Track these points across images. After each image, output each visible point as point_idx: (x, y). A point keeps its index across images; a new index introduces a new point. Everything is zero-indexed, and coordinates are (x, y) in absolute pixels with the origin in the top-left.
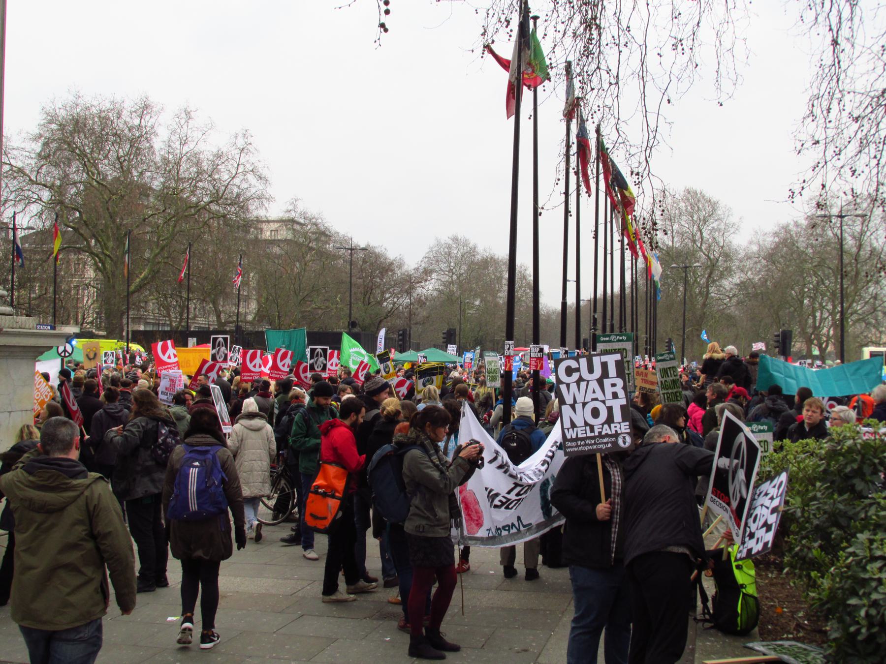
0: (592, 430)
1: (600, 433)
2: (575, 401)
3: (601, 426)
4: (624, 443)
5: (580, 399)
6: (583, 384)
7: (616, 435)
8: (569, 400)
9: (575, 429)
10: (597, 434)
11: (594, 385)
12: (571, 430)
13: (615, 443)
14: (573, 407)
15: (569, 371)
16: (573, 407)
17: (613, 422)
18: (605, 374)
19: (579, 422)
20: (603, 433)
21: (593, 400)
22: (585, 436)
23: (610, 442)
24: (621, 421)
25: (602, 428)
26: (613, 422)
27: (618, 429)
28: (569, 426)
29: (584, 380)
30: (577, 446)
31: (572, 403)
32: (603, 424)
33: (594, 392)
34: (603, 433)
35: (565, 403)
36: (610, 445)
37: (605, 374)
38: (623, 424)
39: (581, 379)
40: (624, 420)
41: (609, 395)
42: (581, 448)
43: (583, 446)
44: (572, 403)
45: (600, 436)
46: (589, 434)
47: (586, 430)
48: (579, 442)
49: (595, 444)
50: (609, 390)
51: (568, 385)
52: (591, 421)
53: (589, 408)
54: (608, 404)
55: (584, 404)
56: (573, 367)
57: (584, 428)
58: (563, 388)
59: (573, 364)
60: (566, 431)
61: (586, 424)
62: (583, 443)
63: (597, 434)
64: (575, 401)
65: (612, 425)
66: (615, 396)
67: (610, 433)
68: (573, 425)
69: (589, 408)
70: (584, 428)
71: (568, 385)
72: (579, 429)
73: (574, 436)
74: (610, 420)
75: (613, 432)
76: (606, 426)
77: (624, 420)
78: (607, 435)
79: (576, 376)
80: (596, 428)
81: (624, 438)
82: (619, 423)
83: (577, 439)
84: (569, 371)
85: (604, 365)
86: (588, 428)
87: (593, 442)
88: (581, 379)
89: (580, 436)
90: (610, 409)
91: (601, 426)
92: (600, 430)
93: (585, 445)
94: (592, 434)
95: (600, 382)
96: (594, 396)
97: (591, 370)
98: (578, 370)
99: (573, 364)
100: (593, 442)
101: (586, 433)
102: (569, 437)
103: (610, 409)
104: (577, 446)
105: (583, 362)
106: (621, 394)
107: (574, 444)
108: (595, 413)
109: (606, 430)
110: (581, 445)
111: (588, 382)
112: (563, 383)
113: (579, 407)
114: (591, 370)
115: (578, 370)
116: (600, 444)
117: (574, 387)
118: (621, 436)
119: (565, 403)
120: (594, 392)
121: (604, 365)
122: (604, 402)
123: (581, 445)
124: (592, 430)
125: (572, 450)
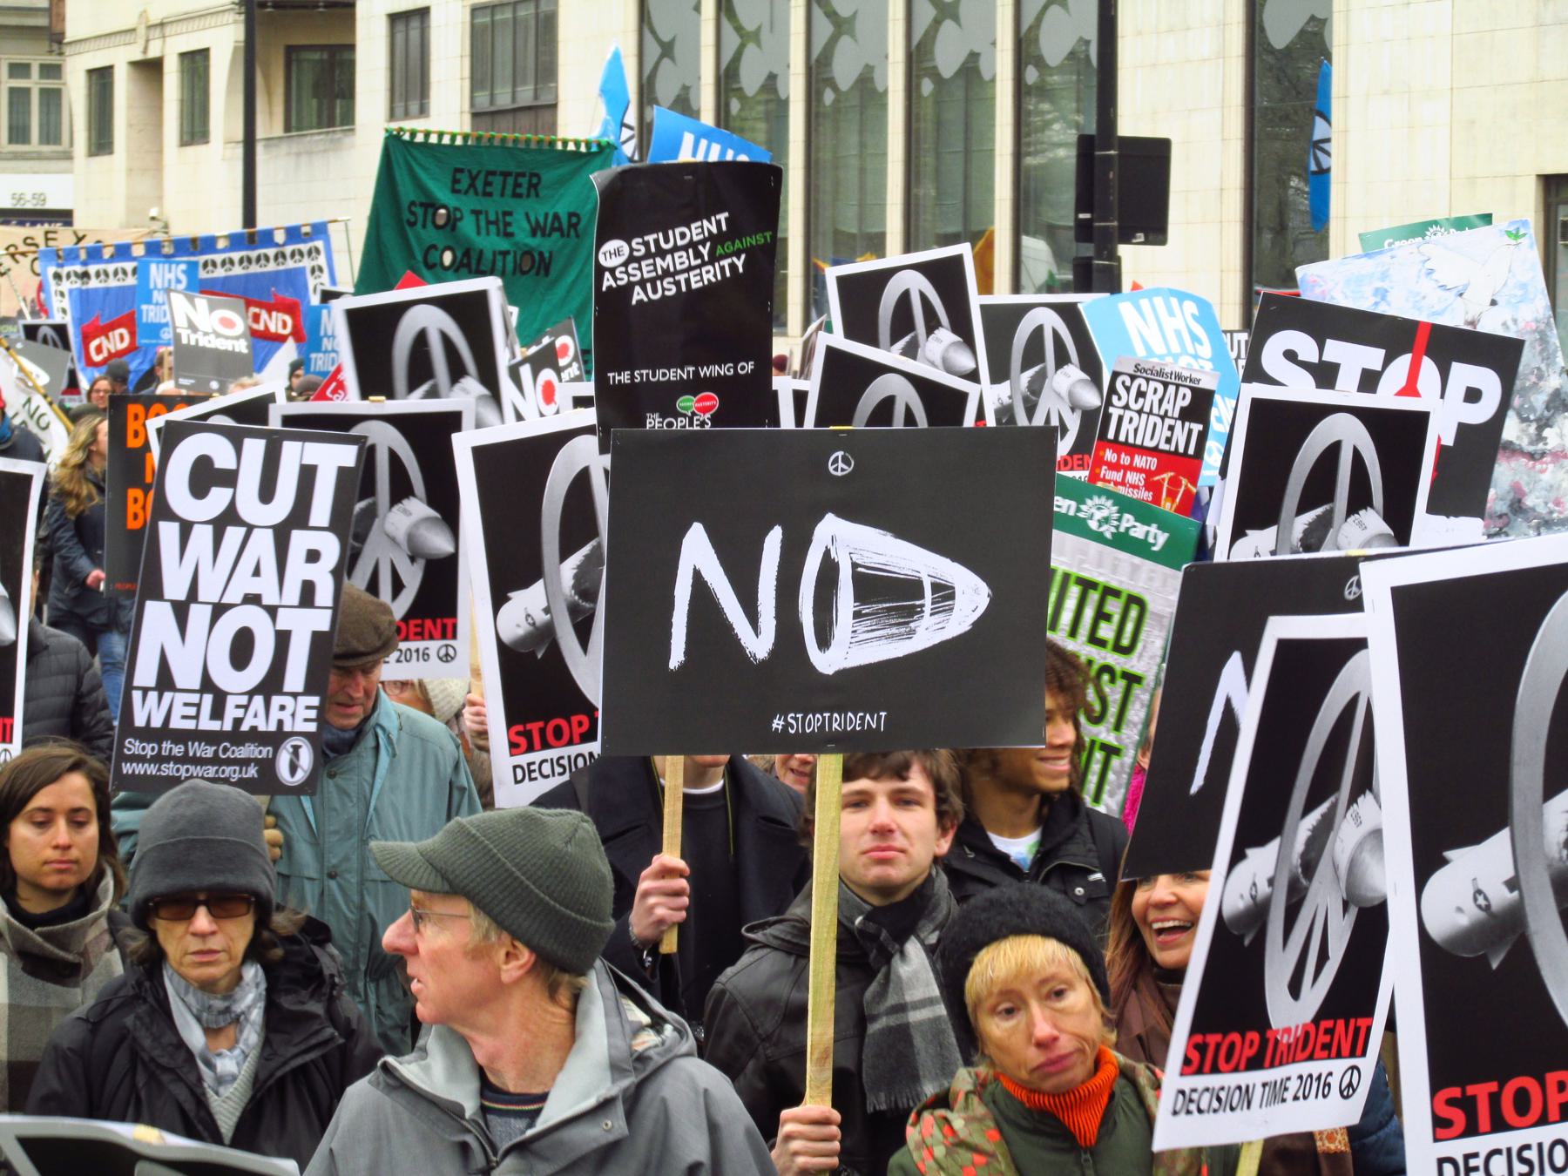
0: (217, 712)
1: (238, 722)
3: (244, 700)
4: (293, 768)
5: (209, 591)
6: (234, 534)
7: (276, 738)
8: (175, 584)
9: (168, 696)
10: (228, 726)
11: (263, 544)
12: (153, 695)
14: (181, 611)
15: (205, 477)
16: (181, 611)
17: (280, 692)
19: (186, 675)
20: (245, 727)
22: (190, 725)
23: (257, 761)
24: (300, 688)
25: (246, 707)
26: (279, 690)
27: (286, 716)
28: (152, 683)
30: (159, 759)
32: (251, 694)
33: (257, 572)
34: (245, 727)
35: (158, 596)
36: (252, 772)
39: (230, 517)
40: (309, 690)
41: (293, 593)
43: (177, 760)
44: (181, 596)
45: (237, 736)
46: (207, 724)
47: (198, 706)
48: (166, 745)
50: (298, 571)
51: (186, 528)
52: (225, 676)
55: (219, 610)
56: (219, 464)
57: (195, 698)
58: (168, 532)
60: (137, 696)
61: (207, 685)
62: (178, 750)
63: (228, 726)
65: (276, 700)
66: (307, 595)
67: (262, 728)
68: (165, 681)
70: (195, 698)
71: (186, 528)
72: (181, 698)
73: (157, 723)
74: (272, 685)
75: (273, 727)
76: (258, 701)
77: (309, 690)
78: (255, 736)
79: (218, 499)
80: (231, 702)
81: (296, 749)
82: (295, 695)
83: (165, 733)
84: (205, 477)
85: (308, 475)
86: (208, 699)
87: (209, 752)
88: (230, 517)
89: (176, 723)
90: (283, 639)
92: (240, 713)
94: (215, 726)
95: (282, 535)
96: (254, 586)
97: (267, 492)
99: (220, 452)
100: (209, 752)
101: (197, 717)
102: (140, 721)
103: (283, 639)
105: (255, 449)
106: (324, 595)
107: (149, 750)
109: (257, 718)
110: (170, 758)
111: (250, 528)
112: (171, 516)
113: (199, 615)
114: (267, 492)
115: (229, 478)
116: (229, 762)
117: (202, 537)
119: (158, 596)
120: (257, 572)
121: (308, 475)
122: (272, 611)
123: (170, 758)
124: (217, 712)
125: (140, 769)
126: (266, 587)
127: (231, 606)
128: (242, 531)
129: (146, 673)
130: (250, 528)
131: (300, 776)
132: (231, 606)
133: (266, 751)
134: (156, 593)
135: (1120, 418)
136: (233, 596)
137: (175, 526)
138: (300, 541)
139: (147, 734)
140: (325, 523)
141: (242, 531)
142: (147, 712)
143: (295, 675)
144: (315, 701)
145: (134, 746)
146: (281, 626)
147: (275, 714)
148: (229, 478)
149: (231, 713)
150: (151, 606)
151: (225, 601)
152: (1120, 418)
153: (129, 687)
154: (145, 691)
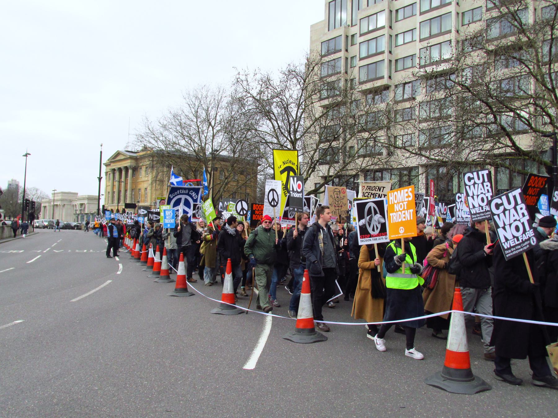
0: (518, 240)
1: (522, 240)
3: (522, 236)
5: (507, 223)
6: (507, 212)
9: (508, 242)
10: (521, 241)
11: (513, 211)
12: (506, 243)
13: (530, 244)
14: (504, 228)
16: (504, 228)
18: (516, 204)
19: (510, 237)
20: (524, 240)
21: (515, 220)
22: (514, 244)
23: (528, 244)
27: (529, 235)
28: (504, 241)
29: (507, 210)
31: (503, 225)
32: (522, 235)
33: (514, 216)
34: (524, 240)
36: (528, 246)
37: (516, 204)
38: (530, 231)
39: (505, 210)
41: (521, 216)
42: (514, 253)
43: (515, 251)
44: (503, 225)
46: (517, 243)
47: (514, 241)
48: (512, 249)
49: (522, 247)
50: (520, 212)
51: (498, 215)
52: (516, 234)
53: (513, 226)
54: (522, 221)
55: (510, 225)
57: (513, 240)
58: (496, 217)
59: (498, 201)
60: (503, 244)
61: (514, 237)
62: (514, 249)
66: (523, 215)
67: (526, 239)
68: (507, 240)
69: (513, 226)
70: (513, 240)
72: (510, 241)
73: (509, 247)
74: (525, 231)
75: (528, 238)
76: (524, 235)
77: (530, 229)
78: (526, 240)
79: (501, 208)
80: (519, 238)
82: (529, 231)
83: (511, 247)
84: (498, 206)
86: (515, 239)
87: (520, 247)
88: (505, 210)
89: (512, 245)
90: (523, 224)
91: (522, 236)
93: (516, 250)
95: (515, 208)
96: (514, 218)
97: (509, 203)
98: (502, 204)
99: (498, 201)
102: (506, 248)
103: (523, 224)
104: (512, 252)
107: (510, 251)
108: (517, 229)
109: (525, 238)
110: (513, 251)
111: (509, 210)
112: (495, 215)
113: (507, 227)
114: (509, 203)
115: (502, 204)
117: (502, 215)
118: (531, 239)
120: (514, 216)
121: (515, 197)
122: (519, 220)
123: (513, 251)
124: (518, 240)
125: (509, 255)
126: (517, 217)
127: (512, 224)
128: (508, 211)
129: (503, 240)
130: (509, 210)
131: (535, 242)
132: (512, 224)
133: (528, 242)
134: (498, 227)
135: (393, 216)
137: (497, 216)
138: (518, 208)
139: (508, 249)
140: (521, 203)
141: (508, 211)
142: (506, 246)
143: (527, 228)
144: (532, 230)
145: (507, 252)
146: (522, 222)
147: (527, 236)
149: (520, 239)
152: (393, 216)
153: (501, 244)
154: (504, 243)
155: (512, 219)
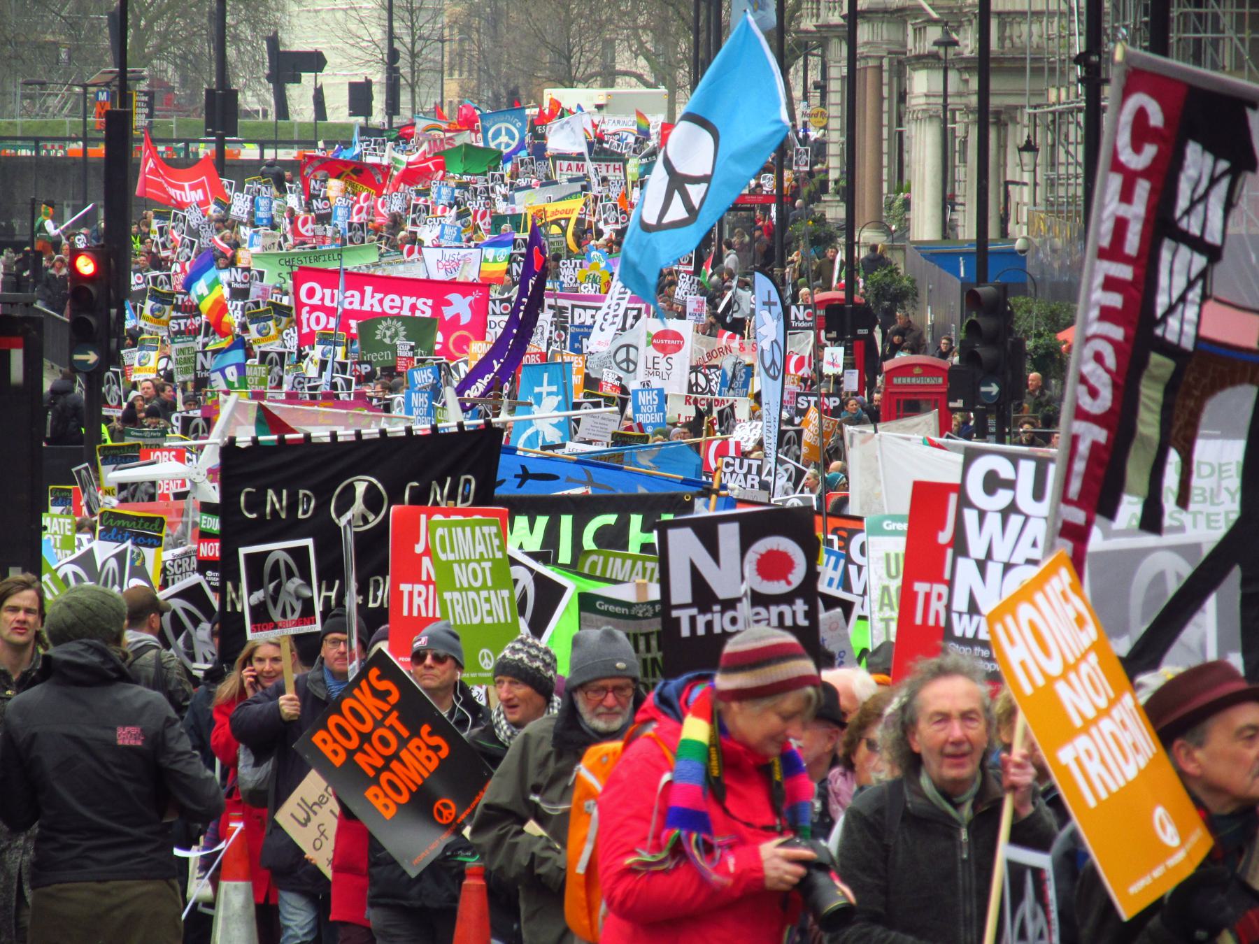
2: (989, 555)
5: (1001, 554)
6: (1016, 521)
8: (977, 547)
9: (976, 618)
12: (966, 618)
14: (982, 566)
15: (993, 483)
16: (982, 566)
31: (982, 556)
33: (1034, 544)
44: (982, 556)
51: (982, 515)
55: (1008, 567)
58: (970, 516)
60: (955, 617)
64: (989, 555)
68: (973, 609)
71: (982, 515)
79: (1003, 498)
84: (993, 483)
99: (1005, 469)
102: (958, 632)
111: (1027, 517)
113: (994, 569)
115: (1011, 485)
117: (993, 520)
128: (1021, 519)
130: (1027, 517)
136: (1018, 558)
139: (963, 641)
141: (1021, 519)
148: (1011, 485)
150: (961, 561)
151: (1013, 561)
154: (960, 614)
155: (1025, 551)
